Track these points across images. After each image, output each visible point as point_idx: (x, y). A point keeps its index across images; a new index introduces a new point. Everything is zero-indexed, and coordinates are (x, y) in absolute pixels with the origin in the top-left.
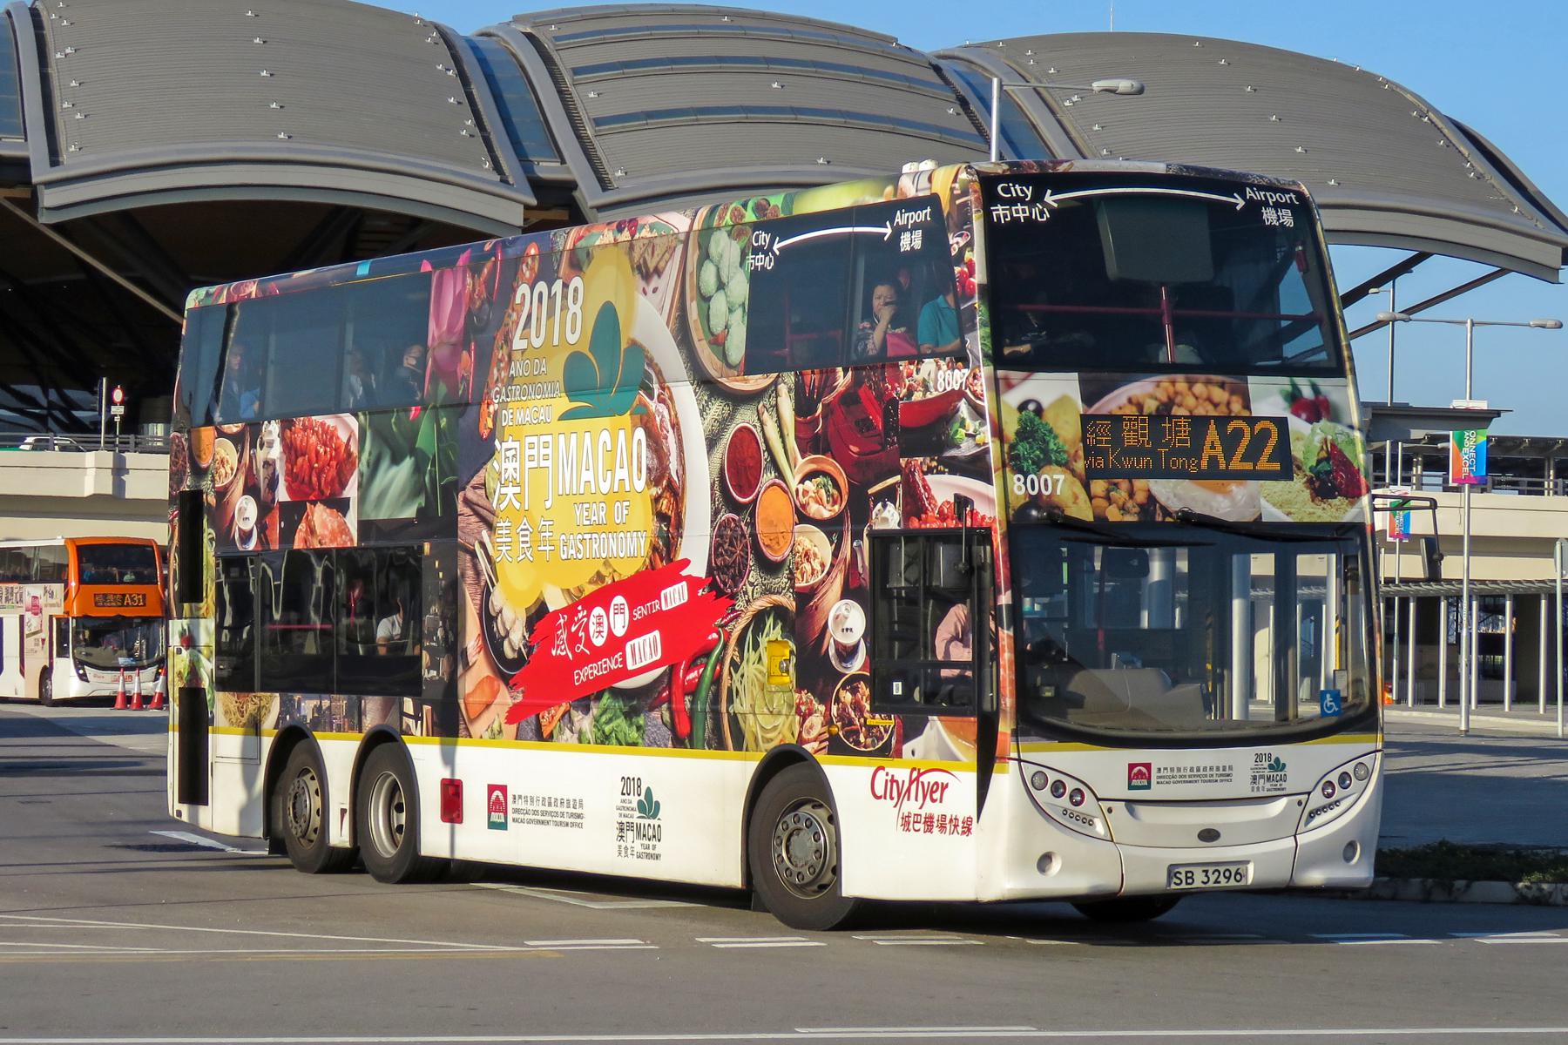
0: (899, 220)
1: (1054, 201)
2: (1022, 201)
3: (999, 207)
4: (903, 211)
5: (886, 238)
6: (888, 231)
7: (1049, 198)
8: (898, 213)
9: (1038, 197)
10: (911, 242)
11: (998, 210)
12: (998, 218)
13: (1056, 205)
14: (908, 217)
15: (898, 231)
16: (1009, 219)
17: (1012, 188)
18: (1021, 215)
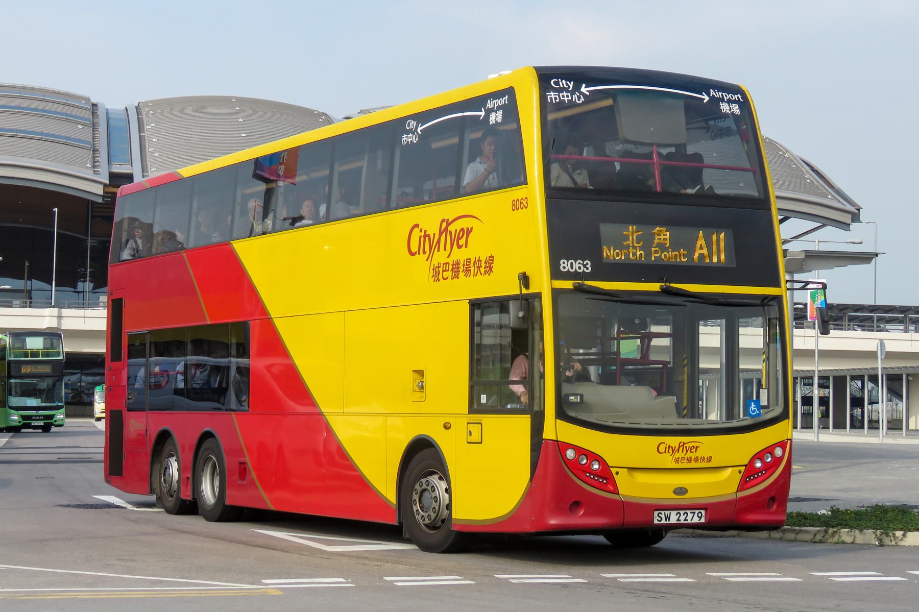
0: (489, 105)
1: (587, 91)
2: (567, 90)
3: (552, 93)
4: (492, 99)
5: (481, 118)
6: (483, 113)
7: (584, 89)
8: (489, 101)
9: (577, 88)
10: (496, 118)
11: (551, 95)
12: (551, 98)
13: (588, 94)
14: (495, 102)
15: (489, 112)
16: (558, 101)
17: (560, 83)
18: (566, 99)
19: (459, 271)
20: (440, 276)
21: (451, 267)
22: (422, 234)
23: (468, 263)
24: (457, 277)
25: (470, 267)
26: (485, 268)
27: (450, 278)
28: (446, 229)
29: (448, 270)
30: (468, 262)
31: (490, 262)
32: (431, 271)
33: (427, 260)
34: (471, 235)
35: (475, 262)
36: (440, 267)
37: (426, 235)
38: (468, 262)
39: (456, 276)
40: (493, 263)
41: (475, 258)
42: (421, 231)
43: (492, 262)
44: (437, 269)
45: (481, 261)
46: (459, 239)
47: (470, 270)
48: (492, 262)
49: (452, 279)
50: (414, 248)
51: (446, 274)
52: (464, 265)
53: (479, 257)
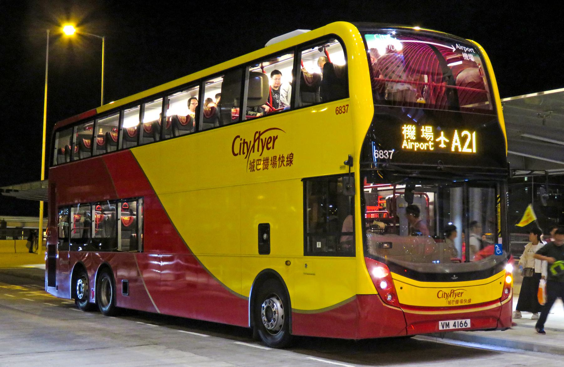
19: (268, 164)
20: (255, 168)
21: (262, 162)
22: (242, 141)
23: (274, 159)
24: (267, 168)
25: (276, 162)
26: (287, 161)
27: (262, 168)
28: (259, 138)
29: (260, 164)
30: (275, 158)
31: (291, 157)
32: (249, 165)
33: (246, 158)
34: (276, 141)
35: (280, 158)
36: (255, 162)
37: (244, 142)
38: (275, 158)
39: (266, 167)
40: (292, 158)
41: (280, 155)
42: (241, 140)
43: (292, 157)
44: (253, 164)
45: (284, 157)
46: (268, 143)
47: (276, 164)
48: (292, 157)
49: (263, 169)
50: (237, 151)
51: (259, 167)
52: (271, 161)
53: (283, 155)
